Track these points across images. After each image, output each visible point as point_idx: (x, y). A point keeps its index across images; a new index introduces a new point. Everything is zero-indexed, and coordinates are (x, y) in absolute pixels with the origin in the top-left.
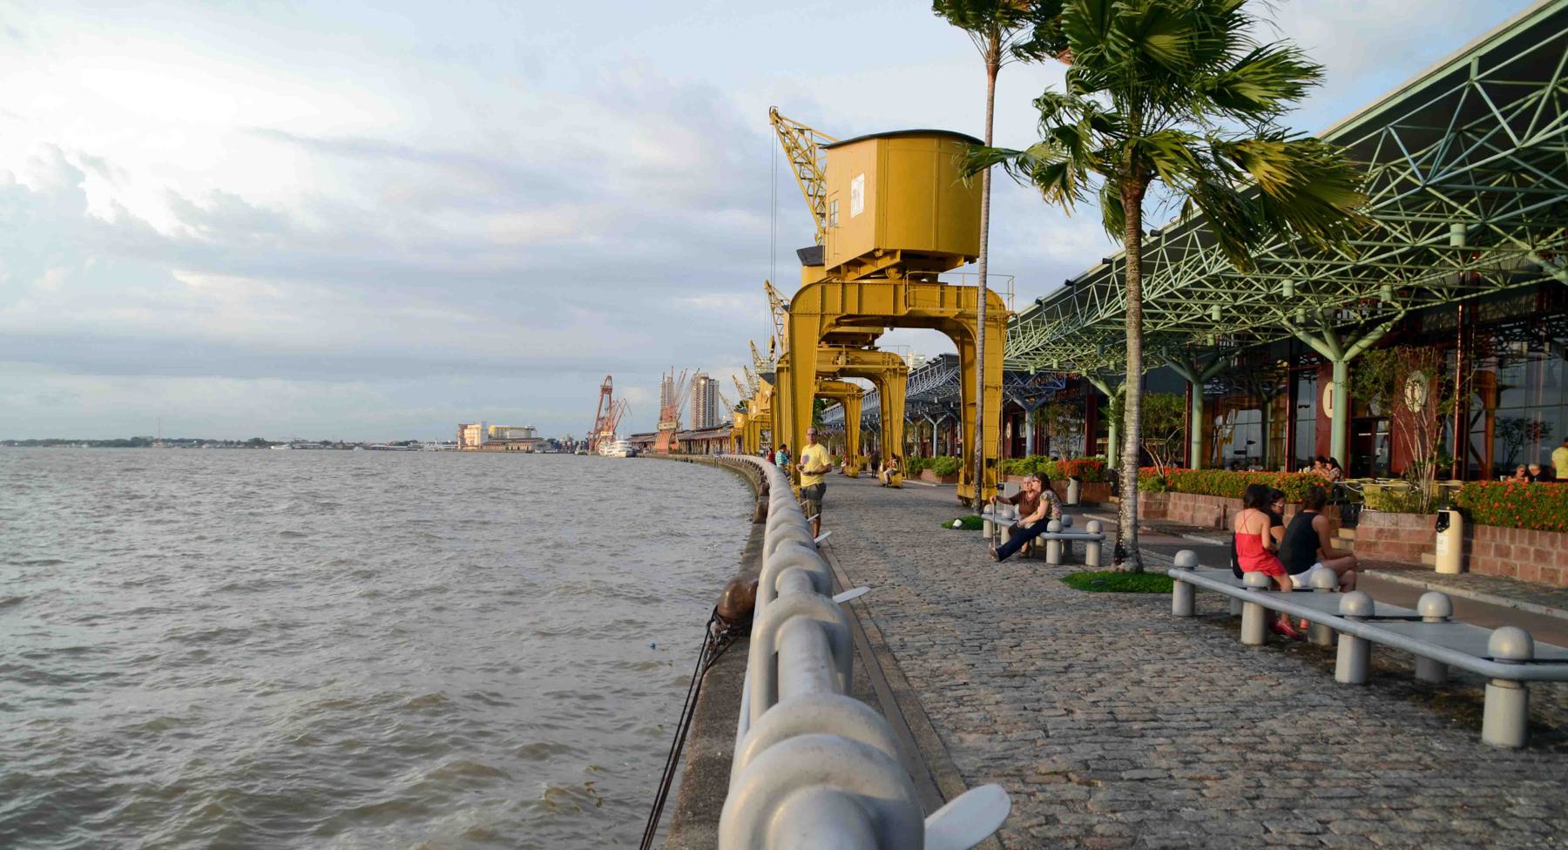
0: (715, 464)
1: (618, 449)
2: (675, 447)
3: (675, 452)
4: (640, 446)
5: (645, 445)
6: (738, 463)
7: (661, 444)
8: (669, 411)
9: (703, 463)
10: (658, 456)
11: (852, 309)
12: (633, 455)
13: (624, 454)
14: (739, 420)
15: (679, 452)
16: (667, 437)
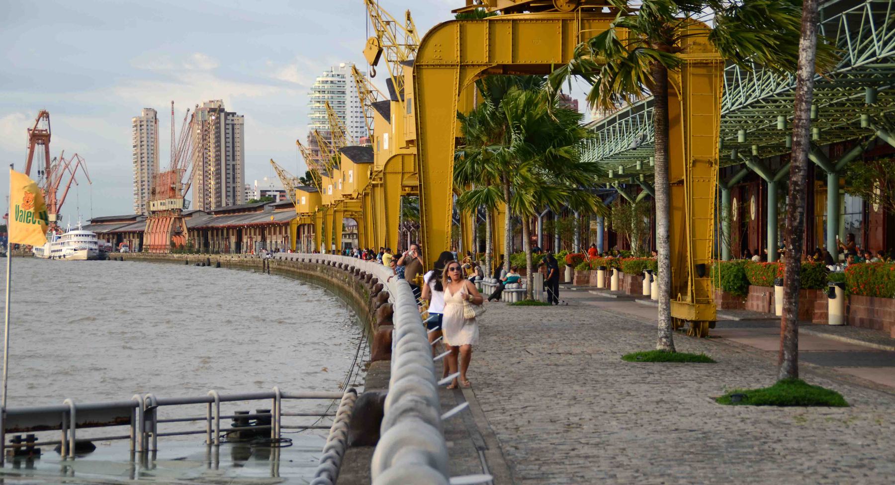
0: (264, 268)
1: (73, 245)
2: (185, 239)
3: (181, 249)
4: (114, 239)
5: (119, 237)
6: (311, 266)
7: (157, 236)
8: (158, 185)
9: (242, 266)
10: (144, 254)
11: (505, 58)
12: (100, 255)
13: (83, 254)
14: (304, 200)
15: (190, 249)
16: (167, 225)
